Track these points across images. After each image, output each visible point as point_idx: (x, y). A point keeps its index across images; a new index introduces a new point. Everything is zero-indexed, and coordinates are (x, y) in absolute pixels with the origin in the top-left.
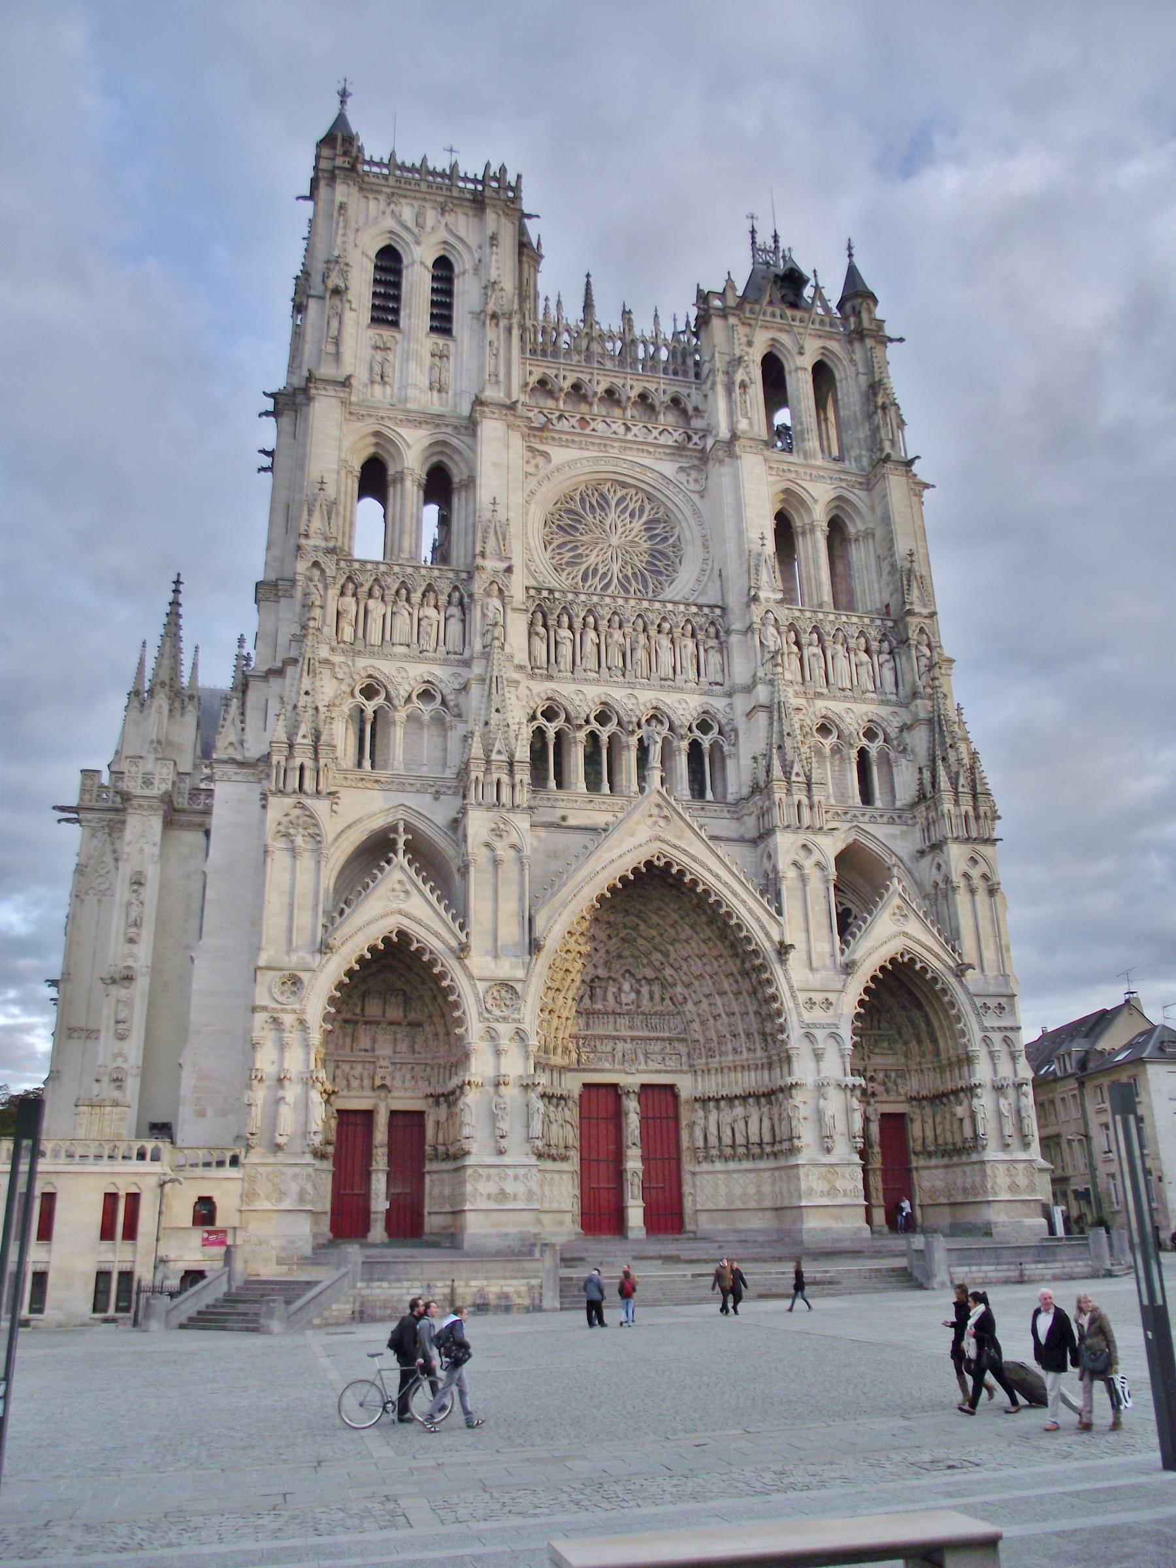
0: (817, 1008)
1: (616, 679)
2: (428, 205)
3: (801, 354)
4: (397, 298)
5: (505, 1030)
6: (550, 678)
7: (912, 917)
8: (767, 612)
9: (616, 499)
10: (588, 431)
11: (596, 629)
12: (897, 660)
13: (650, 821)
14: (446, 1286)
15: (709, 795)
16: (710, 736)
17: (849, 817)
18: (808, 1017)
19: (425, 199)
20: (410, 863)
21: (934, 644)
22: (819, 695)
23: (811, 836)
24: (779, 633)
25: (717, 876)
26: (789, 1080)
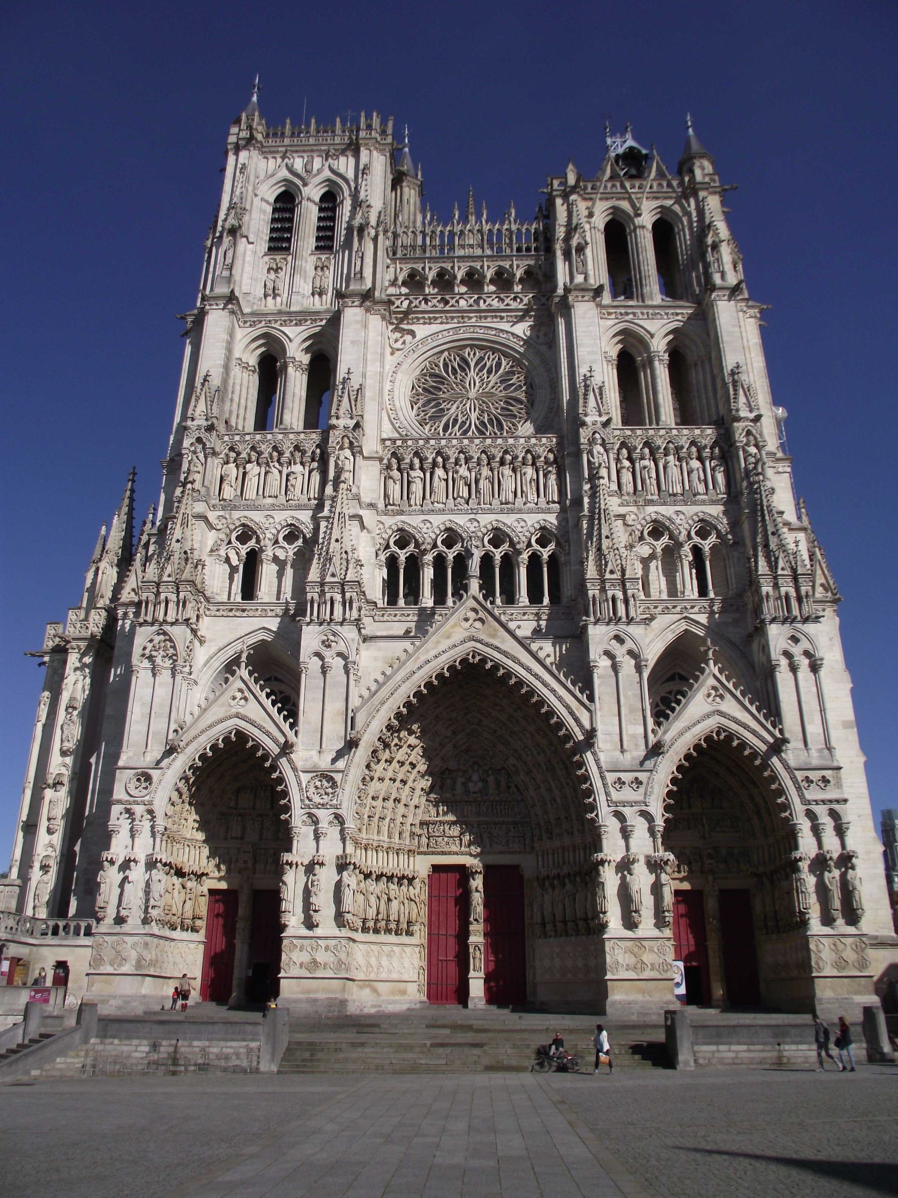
0: (626, 788)
1: (460, 507)
2: (315, 155)
3: (640, 215)
4: (290, 230)
5: (324, 816)
6: (401, 513)
7: (728, 696)
8: (594, 433)
9: (475, 360)
10: (447, 308)
11: (444, 467)
12: (730, 463)
13: (467, 625)
14: (171, 1045)
15: (546, 600)
16: (548, 549)
17: (678, 609)
18: (615, 796)
19: (312, 151)
20: (251, 673)
21: (761, 444)
22: (650, 503)
23: (624, 627)
24: (606, 451)
25: (528, 670)
26: (600, 856)
